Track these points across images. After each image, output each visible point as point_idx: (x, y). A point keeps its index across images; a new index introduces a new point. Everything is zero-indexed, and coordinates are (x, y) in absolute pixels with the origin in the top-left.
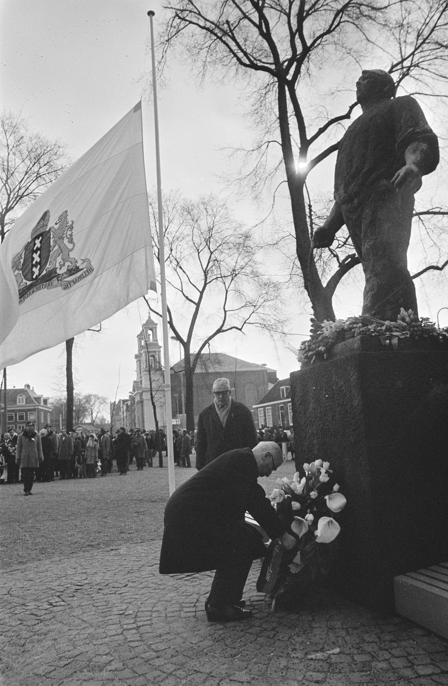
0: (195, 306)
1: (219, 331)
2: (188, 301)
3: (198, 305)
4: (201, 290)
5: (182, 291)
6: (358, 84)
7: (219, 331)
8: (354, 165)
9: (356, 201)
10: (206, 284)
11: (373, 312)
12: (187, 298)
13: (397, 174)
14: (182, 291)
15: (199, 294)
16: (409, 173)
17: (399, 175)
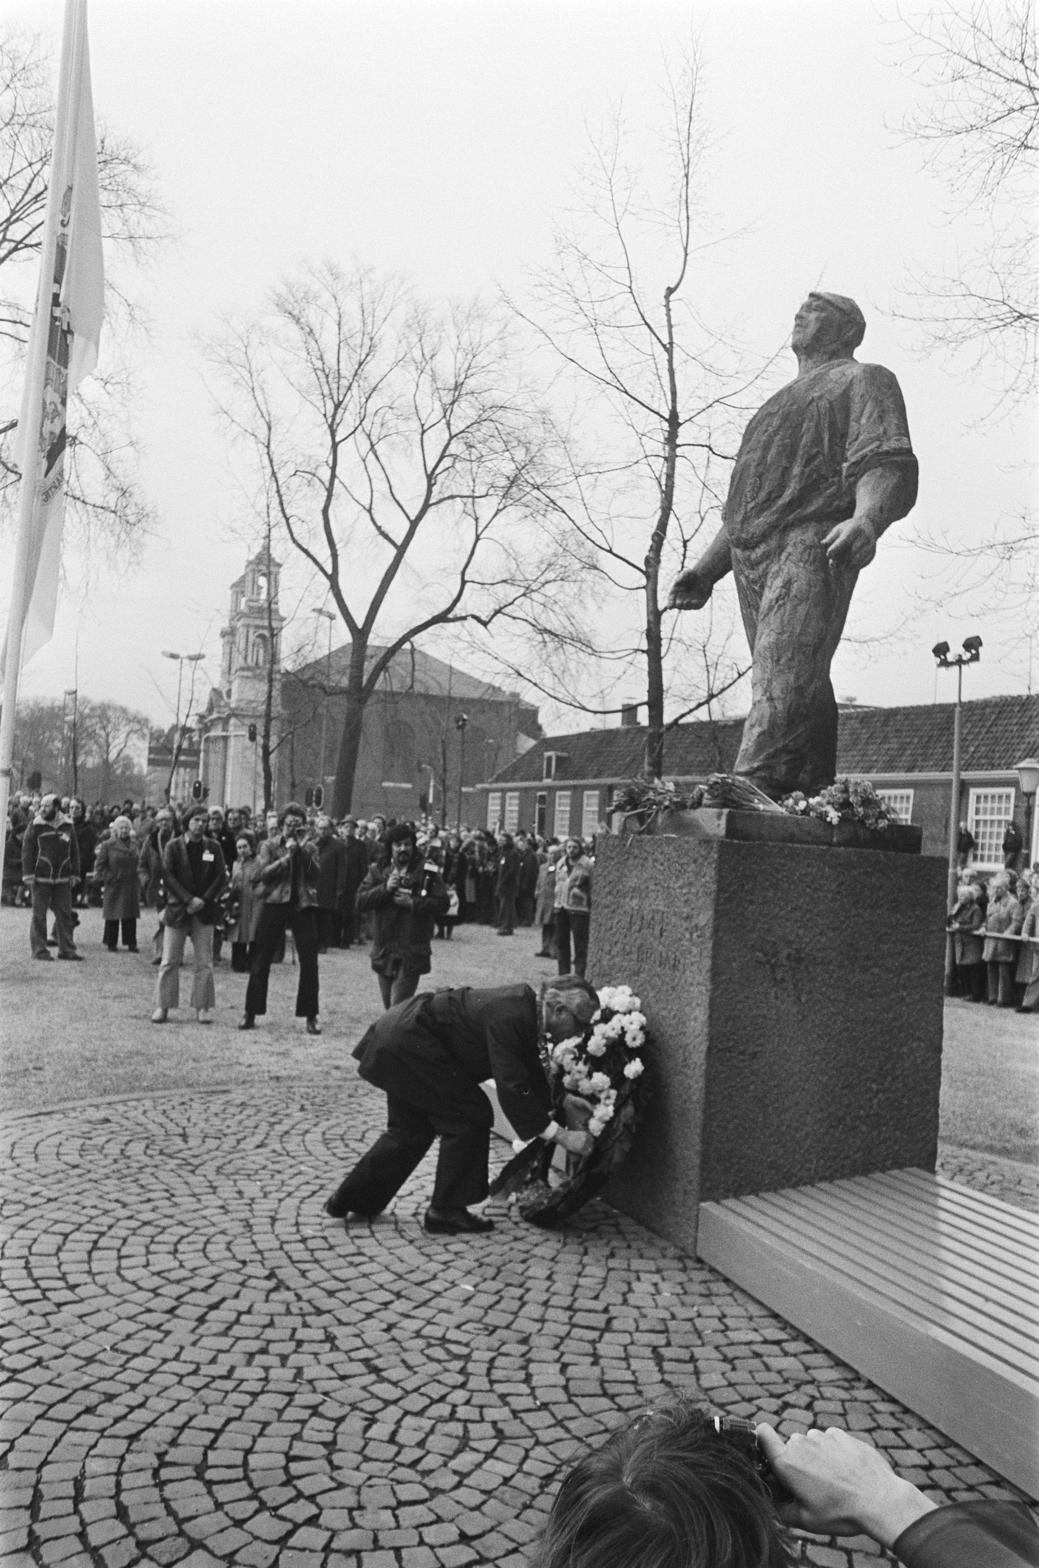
0: (394, 551)
1: (442, 618)
2: (381, 538)
3: (401, 550)
4: (413, 518)
5: (369, 511)
6: (799, 317)
7: (442, 618)
8: (767, 487)
9: (759, 551)
10: (426, 506)
11: (755, 765)
12: (379, 528)
13: (835, 530)
14: (369, 511)
15: (407, 525)
16: (857, 533)
17: (837, 537)
